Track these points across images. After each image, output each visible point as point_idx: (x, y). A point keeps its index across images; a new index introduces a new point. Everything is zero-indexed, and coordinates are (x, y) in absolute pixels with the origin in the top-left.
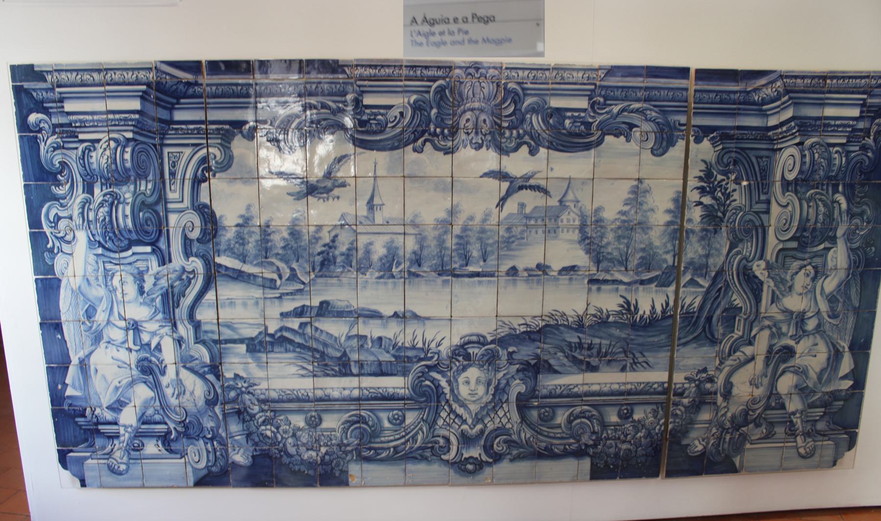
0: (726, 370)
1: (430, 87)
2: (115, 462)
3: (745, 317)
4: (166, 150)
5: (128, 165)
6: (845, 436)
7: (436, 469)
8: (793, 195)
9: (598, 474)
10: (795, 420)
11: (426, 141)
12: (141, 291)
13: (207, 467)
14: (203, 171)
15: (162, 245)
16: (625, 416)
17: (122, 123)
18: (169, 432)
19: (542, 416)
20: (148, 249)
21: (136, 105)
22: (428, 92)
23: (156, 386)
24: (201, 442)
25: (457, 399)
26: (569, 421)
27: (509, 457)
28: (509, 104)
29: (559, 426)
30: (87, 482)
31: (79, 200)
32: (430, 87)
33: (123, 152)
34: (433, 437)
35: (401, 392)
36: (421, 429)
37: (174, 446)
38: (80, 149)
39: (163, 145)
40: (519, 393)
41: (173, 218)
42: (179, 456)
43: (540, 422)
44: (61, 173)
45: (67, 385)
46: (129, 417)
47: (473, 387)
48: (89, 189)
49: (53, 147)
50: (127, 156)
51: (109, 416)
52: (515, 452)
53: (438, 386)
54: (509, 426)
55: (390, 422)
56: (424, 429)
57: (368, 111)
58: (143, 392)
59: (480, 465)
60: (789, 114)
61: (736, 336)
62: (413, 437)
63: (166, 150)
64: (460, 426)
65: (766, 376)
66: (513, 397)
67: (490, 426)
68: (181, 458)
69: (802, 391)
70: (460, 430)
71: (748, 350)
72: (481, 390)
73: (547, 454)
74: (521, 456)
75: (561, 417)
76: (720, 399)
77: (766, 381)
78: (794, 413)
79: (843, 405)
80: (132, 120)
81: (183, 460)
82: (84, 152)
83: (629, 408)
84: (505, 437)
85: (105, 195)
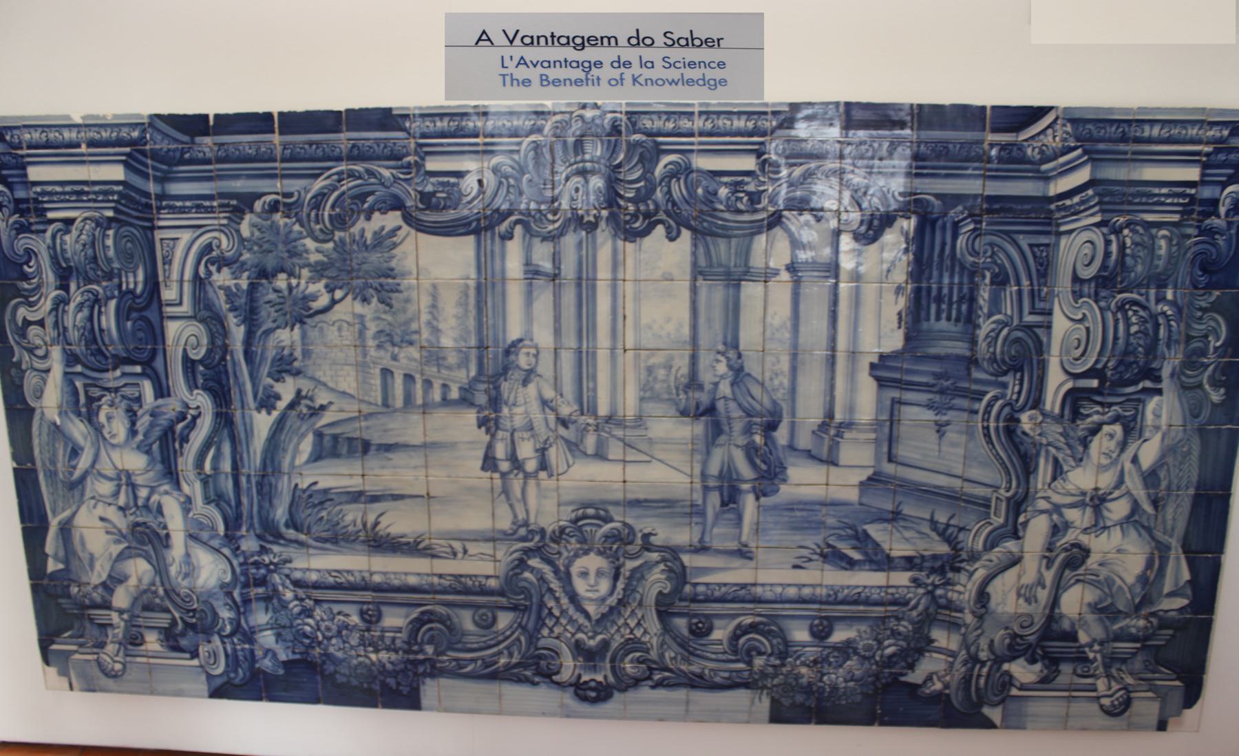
0: (980, 574)
1: (519, 144)
4: (159, 235)
5: (111, 253)
6: (1177, 683)
7: (543, 695)
8: (1091, 302)
9: (778, 716)
10: (1091, 655)
11: (517, 222)
12: (133, 432)
13: (226, 672)
14: (206, 266)
15: (158, 363)
16: (821, 633)
17: (100, 198)
18: (174, 622)
19: (694, 627)
20: (138, 369)
21: (116, 173)
22: (518, 151)
24: (216, 640)
25: (574, 598)
26: (735, 637)
27: (650, 683)
28: (635, 165)
29: (720, 642)
32: (519, 144)
33: (105, 236)
34: (537, 649)
35: (492, 583)
36: (518, 639)
37: (184, 642)
38: (49, 234)
39: (152, 228)
40: (660, 593)
41: (172, 328)
42: (188, 656)
43: (691, 637)
44: (27, 263)
46: (121, 599)
47: (592, 581)
49: (16, 229)
50: (110, 242)
51: (97, 596)
52: (657, 677)
53: (542, 579)
54: (646, 639)
55: (476, 623)
56: (523, 639)
57: (433, 180)
58: (139, 569)
60: (1082, 176)
61: (996, 525)
62: (507, 648)
64: (573, 635)
65: (1044, 587)
66: (651, 598)
67: (617, 641)
68: (192, 658)
69: (1105, 611)
70: (573, 640)
72: (604, 586)
73: (697, 682)
74: (665, 682)
75: (720, 633)
76: (969, 618)
77: (1043, 595)
78: (1090, 646)
79: (1173, 636)
80: (113, 193)
81: (195, 662)
84: (638, 654)
85: (82, 293)
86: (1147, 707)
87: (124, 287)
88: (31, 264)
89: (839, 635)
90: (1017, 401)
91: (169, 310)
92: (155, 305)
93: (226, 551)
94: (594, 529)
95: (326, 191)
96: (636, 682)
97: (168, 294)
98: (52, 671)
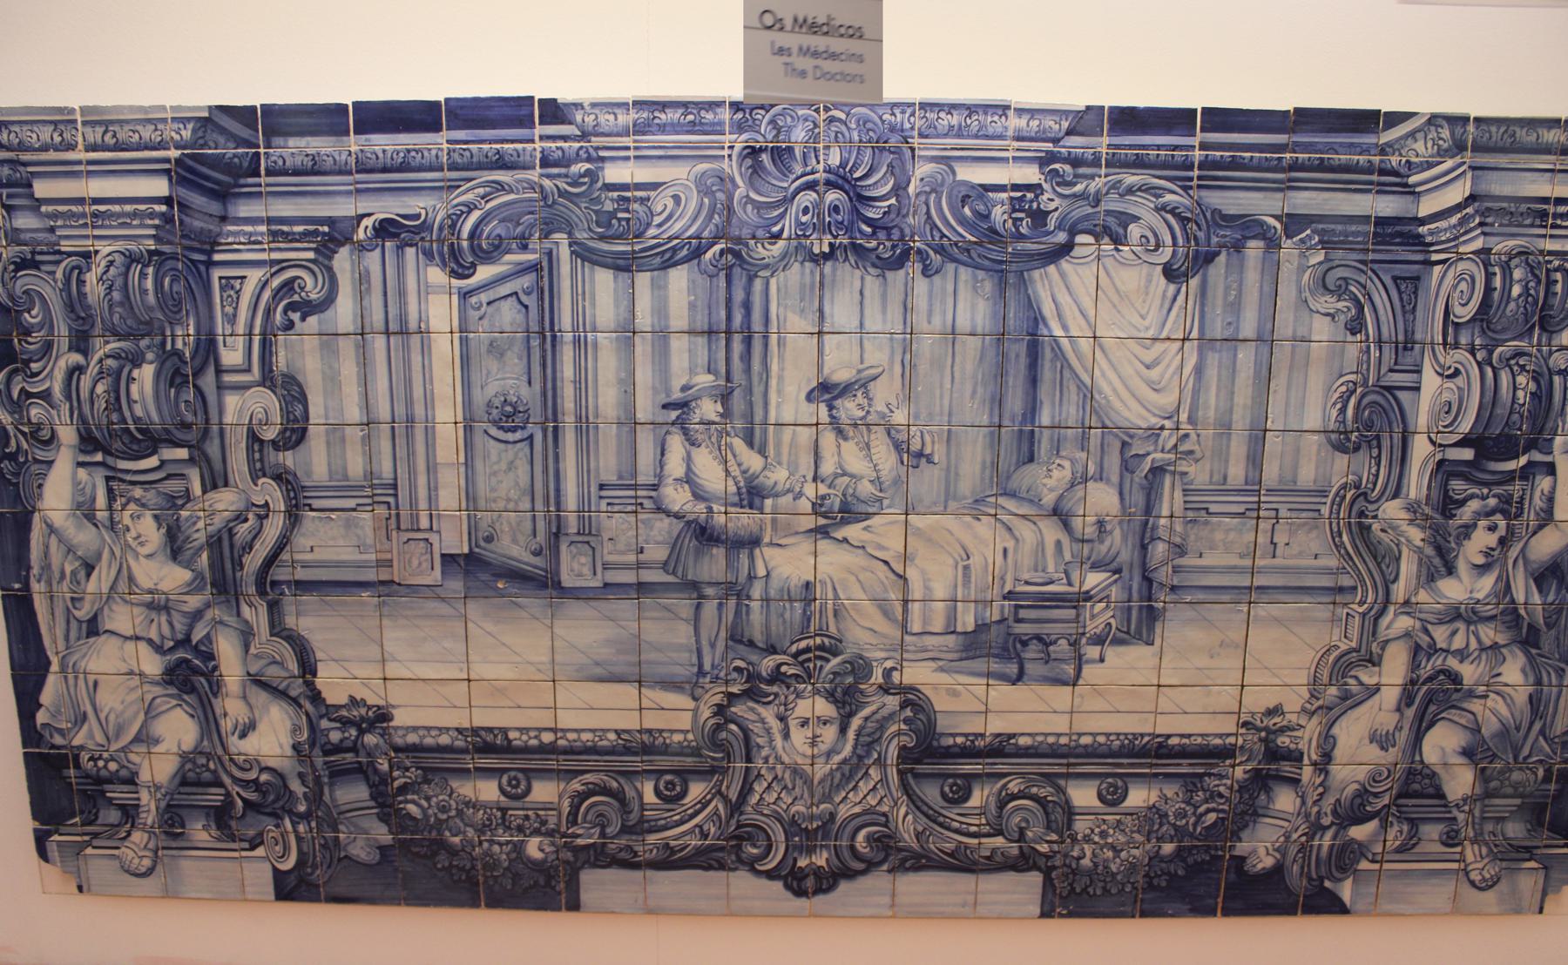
2: (131, 854)
3: (1361, 610)
4: (217, 273)
15: (213, 449)
16: (1112, 797)
23: (209, 721)
30: (85, 888)
31: (62, 363)
39: (210, 264)
40: (903, 749)
41: (232, 401)
45: (40, 706)
46: (158, 769)
48: (81, 343)
50: (149, 284)
59: (825, 882)
61: (1343, 647)
63: (217, 273)
71: (1368, 677)
77: (1403, 737)
80: (152, 215)
82: (67, 279)
83: (1120, 783)
86: (1528, 881)
87: (169, 347)
88: (34, 313)
89: (1138, 797)
90: (1373, 490)
91: (228, 378)
92: (211, 370)
93: (308, 706)
94: (819, 663)
95: (464, 209)
96: (870, 866)
97: (231, 355)
98: (52, 872)
